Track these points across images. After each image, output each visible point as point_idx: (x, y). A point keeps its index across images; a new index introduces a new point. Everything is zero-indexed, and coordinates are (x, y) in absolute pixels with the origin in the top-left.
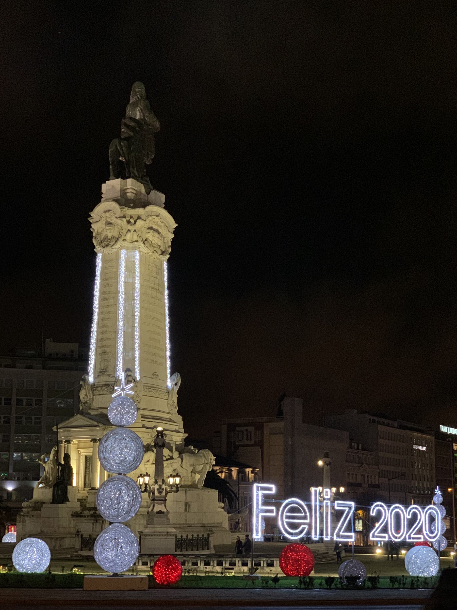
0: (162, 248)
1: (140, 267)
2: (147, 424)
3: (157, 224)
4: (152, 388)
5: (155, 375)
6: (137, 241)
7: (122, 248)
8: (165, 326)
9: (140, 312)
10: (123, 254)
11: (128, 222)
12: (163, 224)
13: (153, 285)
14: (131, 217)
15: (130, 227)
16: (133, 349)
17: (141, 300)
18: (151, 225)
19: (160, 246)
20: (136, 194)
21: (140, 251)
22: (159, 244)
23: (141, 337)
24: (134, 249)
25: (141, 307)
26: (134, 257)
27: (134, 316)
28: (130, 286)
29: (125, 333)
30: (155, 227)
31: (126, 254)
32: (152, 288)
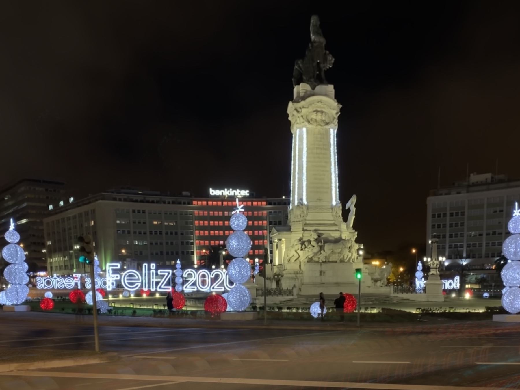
0: (327, 121)
1: (307, 137)
2: (309, 228)
3: (320, 107)
4: (316, 207)
5: (320, 200)
6: (303, 122)
7: (297, 128)
8: (331, 169)
9: (307, 164)
10: (298, 131)
11: (298, 112)
12: (325, 106)
13: (317, 146)
14: (300, 108)
15: (299, 115)
16: (302, 187)
17: (307, 157)
18: (315, 109)
19: (323, 121)
20: (305, 92)
21: (307, 128)
22: (324, 119)
23: (307, 179)
24: (303, 127)
25: (308, 162)
26: (303, 132)
27: (303, 167)
28: (301, 150)
29: (298, 178)
30: (319, 109)
31: (299, 131)
32: (317, 148)
